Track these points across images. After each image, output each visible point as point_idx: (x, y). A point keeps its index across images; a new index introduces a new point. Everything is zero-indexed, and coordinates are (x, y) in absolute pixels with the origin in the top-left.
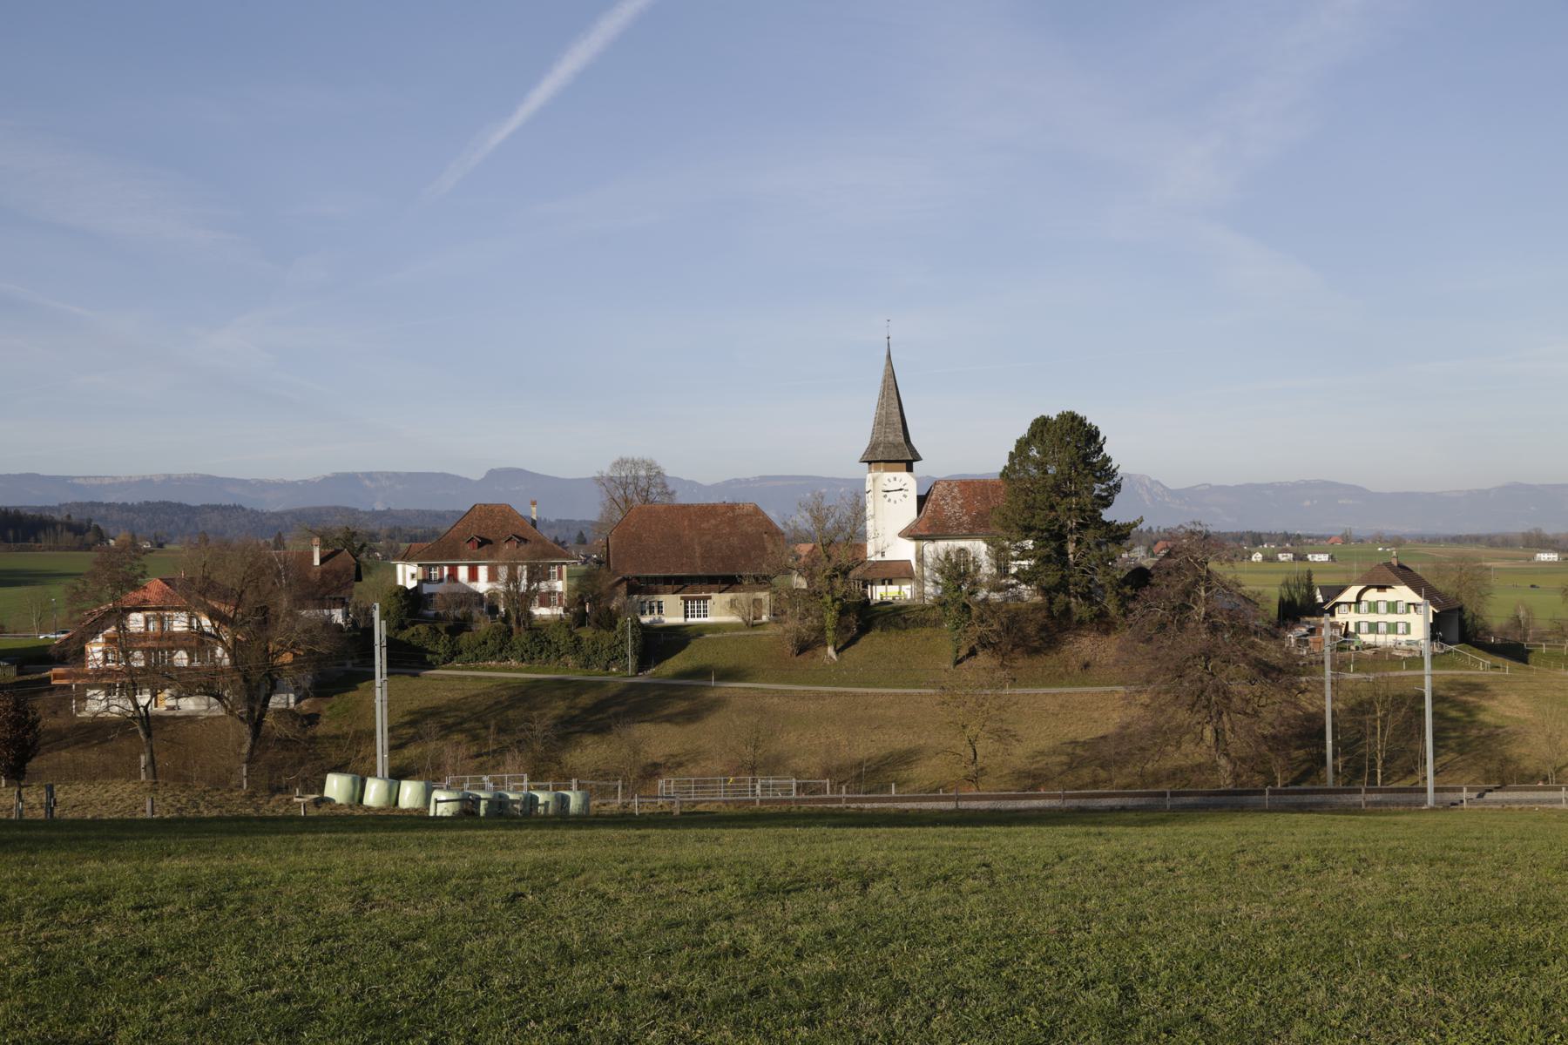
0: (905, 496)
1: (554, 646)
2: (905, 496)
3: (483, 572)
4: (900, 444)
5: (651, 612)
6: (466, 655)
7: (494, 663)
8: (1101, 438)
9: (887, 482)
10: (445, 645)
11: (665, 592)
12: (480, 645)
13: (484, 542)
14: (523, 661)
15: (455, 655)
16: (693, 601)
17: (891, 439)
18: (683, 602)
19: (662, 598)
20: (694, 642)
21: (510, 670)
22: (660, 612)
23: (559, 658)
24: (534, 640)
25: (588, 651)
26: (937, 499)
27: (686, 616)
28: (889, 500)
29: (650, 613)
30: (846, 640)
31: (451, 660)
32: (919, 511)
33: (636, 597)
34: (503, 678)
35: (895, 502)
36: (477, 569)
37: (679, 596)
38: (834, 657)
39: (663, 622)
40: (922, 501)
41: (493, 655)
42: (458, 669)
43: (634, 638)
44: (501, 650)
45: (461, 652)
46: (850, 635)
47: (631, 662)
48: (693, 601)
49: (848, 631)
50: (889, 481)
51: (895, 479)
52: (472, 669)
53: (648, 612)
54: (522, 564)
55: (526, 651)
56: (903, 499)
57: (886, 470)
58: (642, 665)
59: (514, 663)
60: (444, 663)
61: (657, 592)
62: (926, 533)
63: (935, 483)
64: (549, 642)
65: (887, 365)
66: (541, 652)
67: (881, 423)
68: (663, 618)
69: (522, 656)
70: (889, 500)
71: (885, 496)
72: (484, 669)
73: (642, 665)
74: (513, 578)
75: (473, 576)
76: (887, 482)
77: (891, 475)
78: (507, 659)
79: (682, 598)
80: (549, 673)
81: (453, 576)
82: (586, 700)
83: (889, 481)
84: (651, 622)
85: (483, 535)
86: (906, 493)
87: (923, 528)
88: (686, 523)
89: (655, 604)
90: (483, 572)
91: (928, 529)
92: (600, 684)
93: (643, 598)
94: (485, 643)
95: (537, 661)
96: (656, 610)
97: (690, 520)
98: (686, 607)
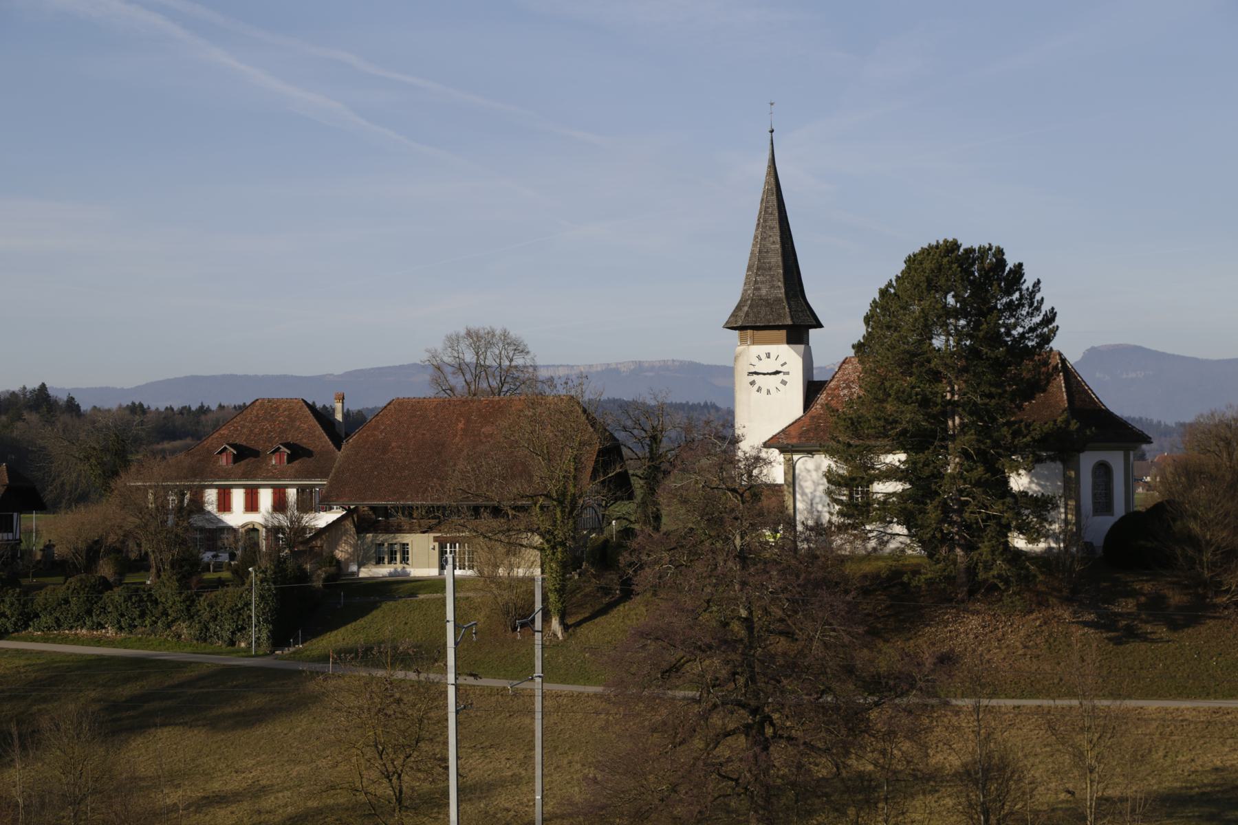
0: (784, 383)
1: (160, 607)
2: (784, 383)
3: (238, 497)
4: (778, 300)
5: (392, 560)
6: (46, 619)
7: (84, 631)
8: (1028, 283)
9: (755, 361)
10: (12, 604)
11: (411, 531)
12: (59, 605)
13: (243, 453)
14: (121, 629)
15: (31, 620)
16: (453, 545)
17: (764, 292)
18: (437, 544)
19: (407, 538)
20: (387, 606)
21: (98, 642)
22: (405, 559)
23: (169, 626)
24: (130, 597)
25: (206, 616)
26: (837, 387)
27: (442, 567)
28: (759, 390)
29: (390, 562)
30: (597, 608)
31: (26, 626)
32: (807, 405)
33: (370, 535)
34: (50, 653)
35: (768, 392)
36: (229, 494)
37: (432, 535)
38: (560, 635)
39: (408, 575)
40: (812, 389)
41: (79, 620)
42: (34, 640)
43: (262, 597)
44: (89, 613)
45: (37, 616)
46: (607, 600)
47: (257, 633)
48: (453, 545)
49: (607, 594)
50: (759, 358)
51: (768, 356)
52: (54, 641)
53: (386, 560)
54: (292, 486)
55: (122, 615)
56: (781, 386)
57: (753, 343)
58: (279, 639)
59: (111, 632)
60: (16, 631)
61: (399, 530)
62: (795, 441)
63: (844, 362)
64: (156, 602)
65: (769, 167)
66: (142, 615)
67: (758, 266)
68: (408, 569)
69: (119, 622)
70: (759, 390)
71: (753, 383)
72: (65, 640)
73: (279, 639)
74: (280, 504)
75: (225, 505)
76: (755, 361)
77: (761, 349)
78: (100, 626)
79: (436, 539)
80: (146, 648)
81: (198, 505)
82: (127, 691)
83: (759, 358)
84: (391, 575)
85: (241, 441)
86: (786, 378)
87: (793, 433)
88: (461, 425)
89: (397, 547)
90: (238, 497)
91: (801, 435)
92: (179, 666)
93: (381, 538)
94: (67, 602)
95: (140, 629)
96: (398, 556)
97: (468, 421)
98: (442, 553)
